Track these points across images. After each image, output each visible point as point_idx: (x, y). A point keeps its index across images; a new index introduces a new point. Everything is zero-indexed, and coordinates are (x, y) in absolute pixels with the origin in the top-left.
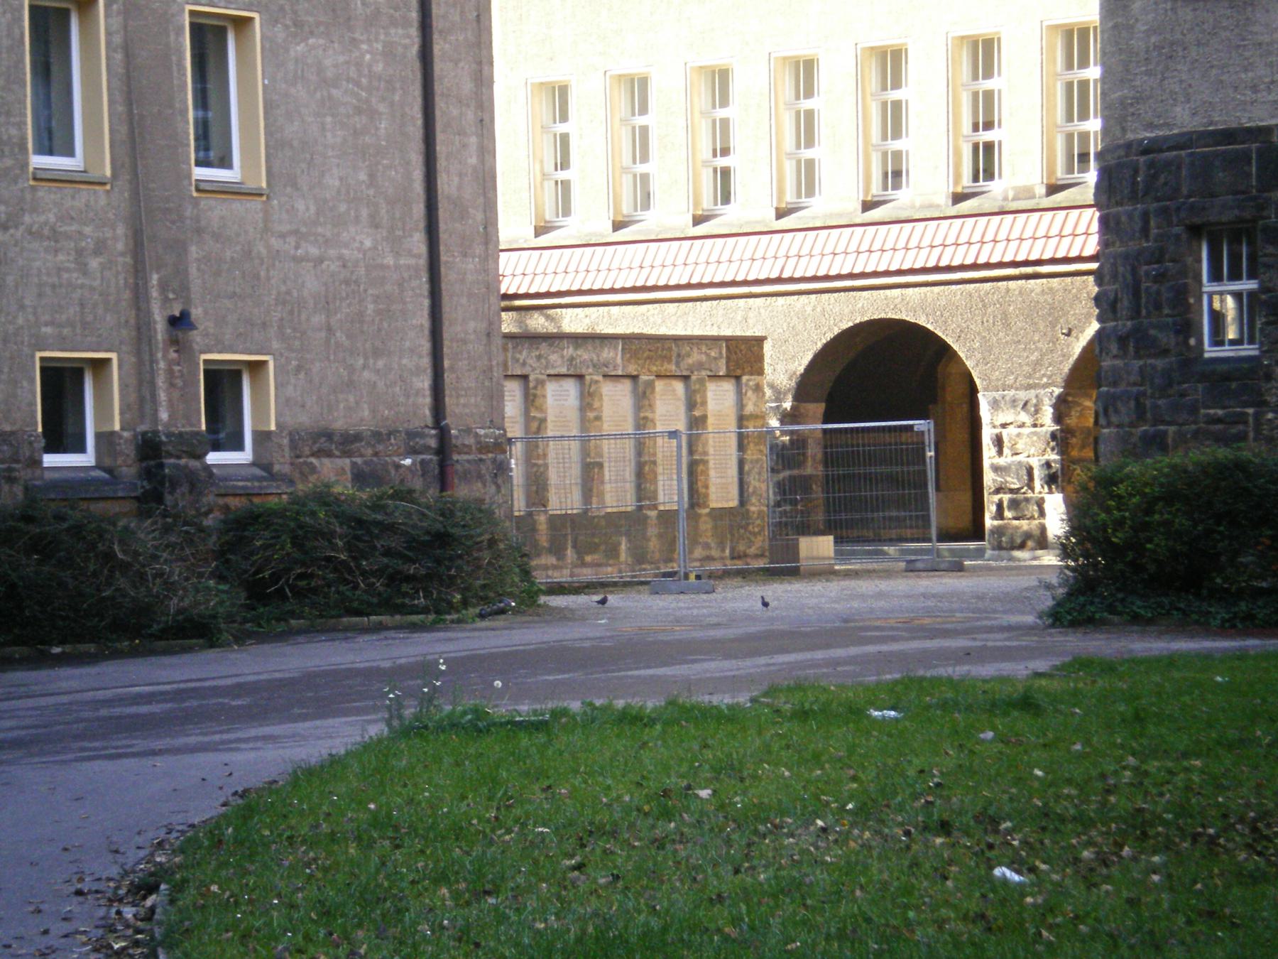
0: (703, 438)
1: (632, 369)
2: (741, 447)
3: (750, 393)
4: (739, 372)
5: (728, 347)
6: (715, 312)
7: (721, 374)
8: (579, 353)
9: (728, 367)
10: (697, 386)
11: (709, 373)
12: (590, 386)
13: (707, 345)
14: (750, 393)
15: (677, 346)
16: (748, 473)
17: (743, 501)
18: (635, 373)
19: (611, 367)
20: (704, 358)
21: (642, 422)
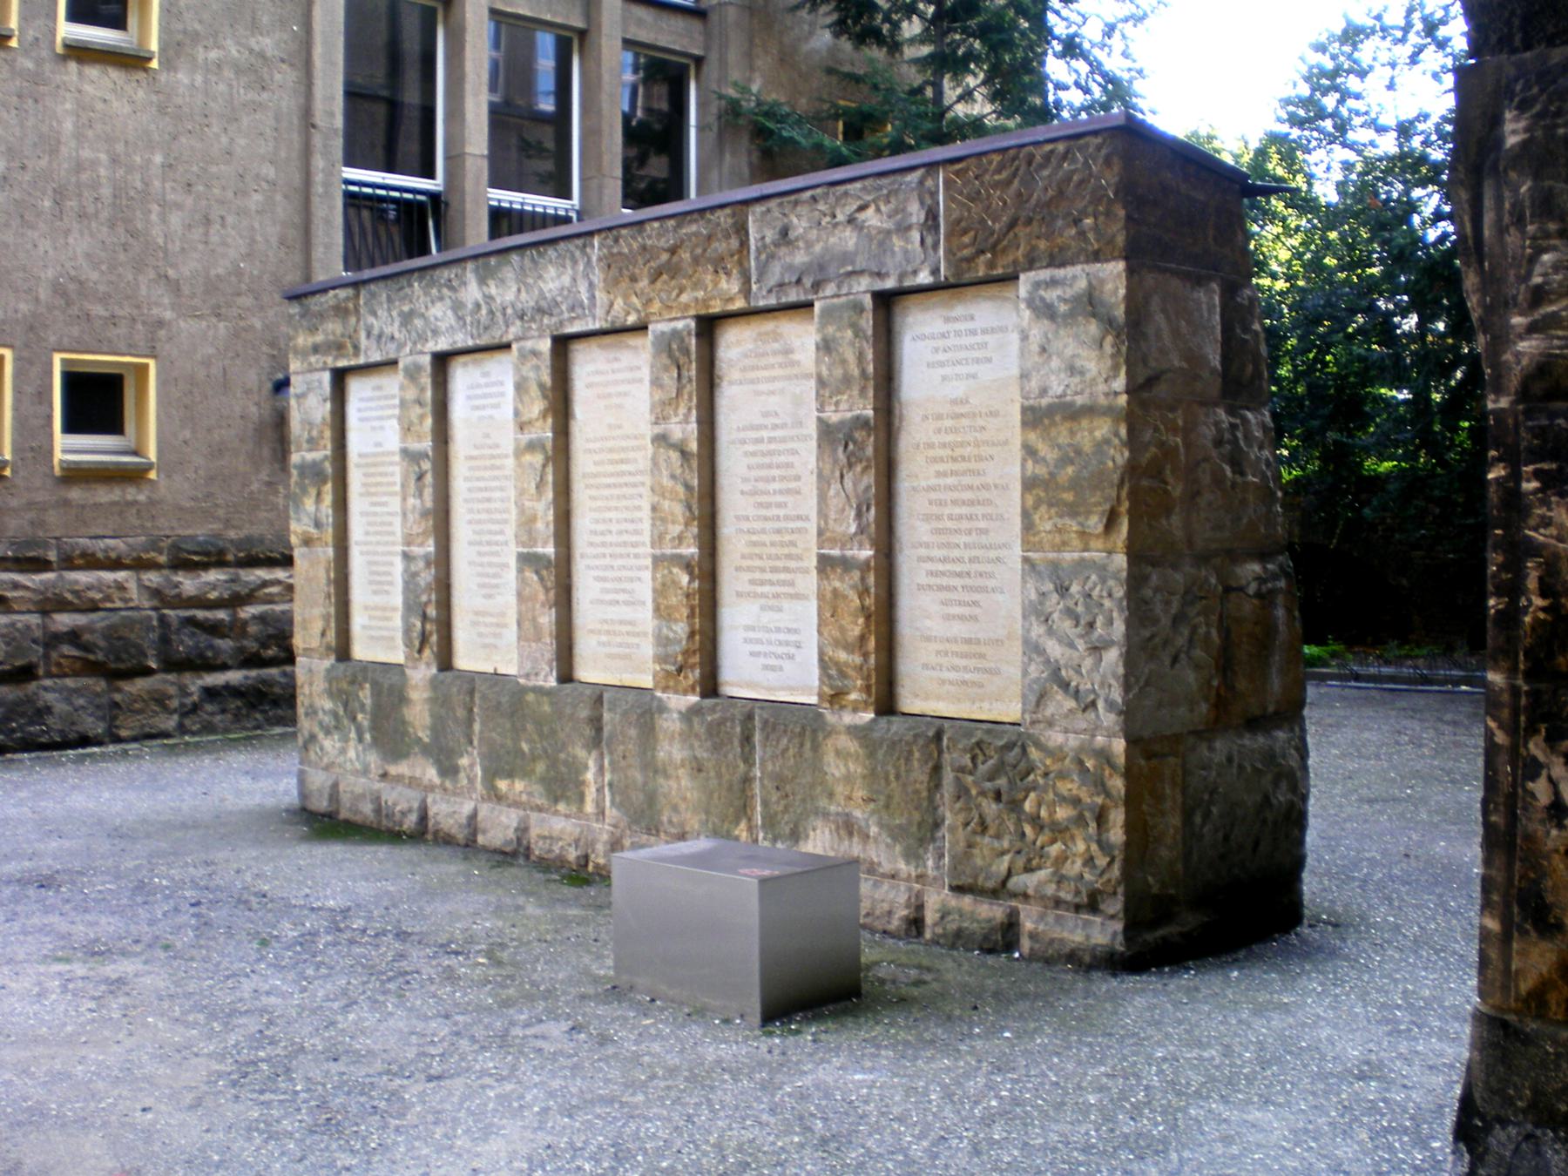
18: (632, 319)
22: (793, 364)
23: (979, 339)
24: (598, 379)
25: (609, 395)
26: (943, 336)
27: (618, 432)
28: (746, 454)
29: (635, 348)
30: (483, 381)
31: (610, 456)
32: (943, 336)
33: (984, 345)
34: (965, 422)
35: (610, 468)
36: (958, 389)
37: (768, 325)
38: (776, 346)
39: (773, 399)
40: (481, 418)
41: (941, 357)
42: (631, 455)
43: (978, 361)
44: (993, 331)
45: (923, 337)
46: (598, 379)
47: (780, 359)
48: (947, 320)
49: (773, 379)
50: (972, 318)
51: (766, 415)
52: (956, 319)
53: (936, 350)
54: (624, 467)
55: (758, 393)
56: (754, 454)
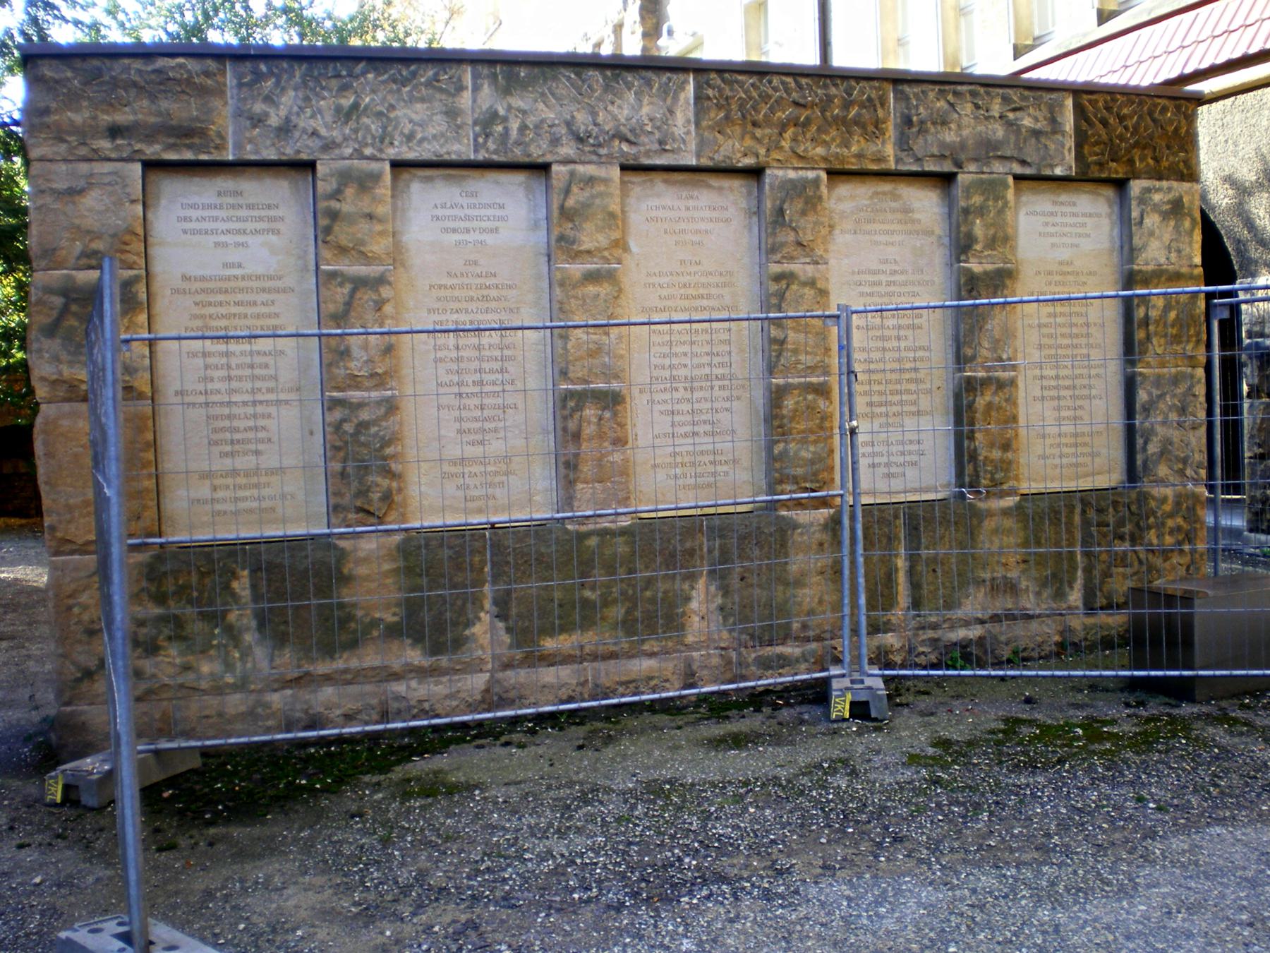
0: (994, 324)
1: (733, 149)
2: (1130, 349)
3: (1152, 220)
4: (1116, 169)
5: (1079, 110)
6: (1229, 118)
7: (1058, 171)
8: (517, 102)
9: (1079, 157)
10: (977, 200)
11: (1018, 169)
12: (567, 192)
13: (1006, 100)
14: (1152, 220)
15: (902, 97)
16: (1147, 410)
17: (1132, 473)
18: (749, 161)
19: (649, 143)
20: (999, 131)
21: (774, 287)
22: (913, 221)
23: (1080, 220)
24: (661, 214)
25: (682, 231)
26: (1052, 214)
27: (693, 269)
28: (862, 294)
29: (720, 189)
30: (465, 201)
31: (682, 291)
32: (1052, 214)
33: (1084, 225)
34: (1071, 278)
35: (686, 303)
36: (1065, 254)
37: (886, 187)
38: (894, 205)
39: (890, 249)
40: (458, 244)
41: (1051, 230)
42: (714, 291)
43: (1080, 235)
44: (1091, 215)
45: (1035, 213)
46: (661, 214)
47: (899, 216)
48: (1055, 203)
49: (893, 232)
50: (1074, 204)
51: (886, 262)
52: (1062, 204)
53: (1047, 224)
54: (705, 303)
55: (877, 243)
56: (871, 295)
